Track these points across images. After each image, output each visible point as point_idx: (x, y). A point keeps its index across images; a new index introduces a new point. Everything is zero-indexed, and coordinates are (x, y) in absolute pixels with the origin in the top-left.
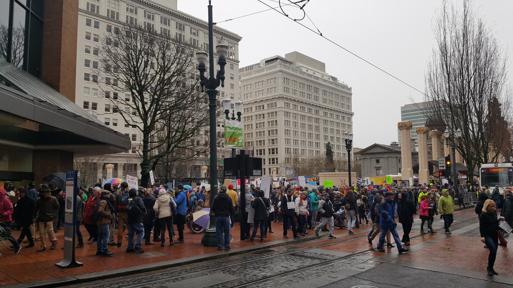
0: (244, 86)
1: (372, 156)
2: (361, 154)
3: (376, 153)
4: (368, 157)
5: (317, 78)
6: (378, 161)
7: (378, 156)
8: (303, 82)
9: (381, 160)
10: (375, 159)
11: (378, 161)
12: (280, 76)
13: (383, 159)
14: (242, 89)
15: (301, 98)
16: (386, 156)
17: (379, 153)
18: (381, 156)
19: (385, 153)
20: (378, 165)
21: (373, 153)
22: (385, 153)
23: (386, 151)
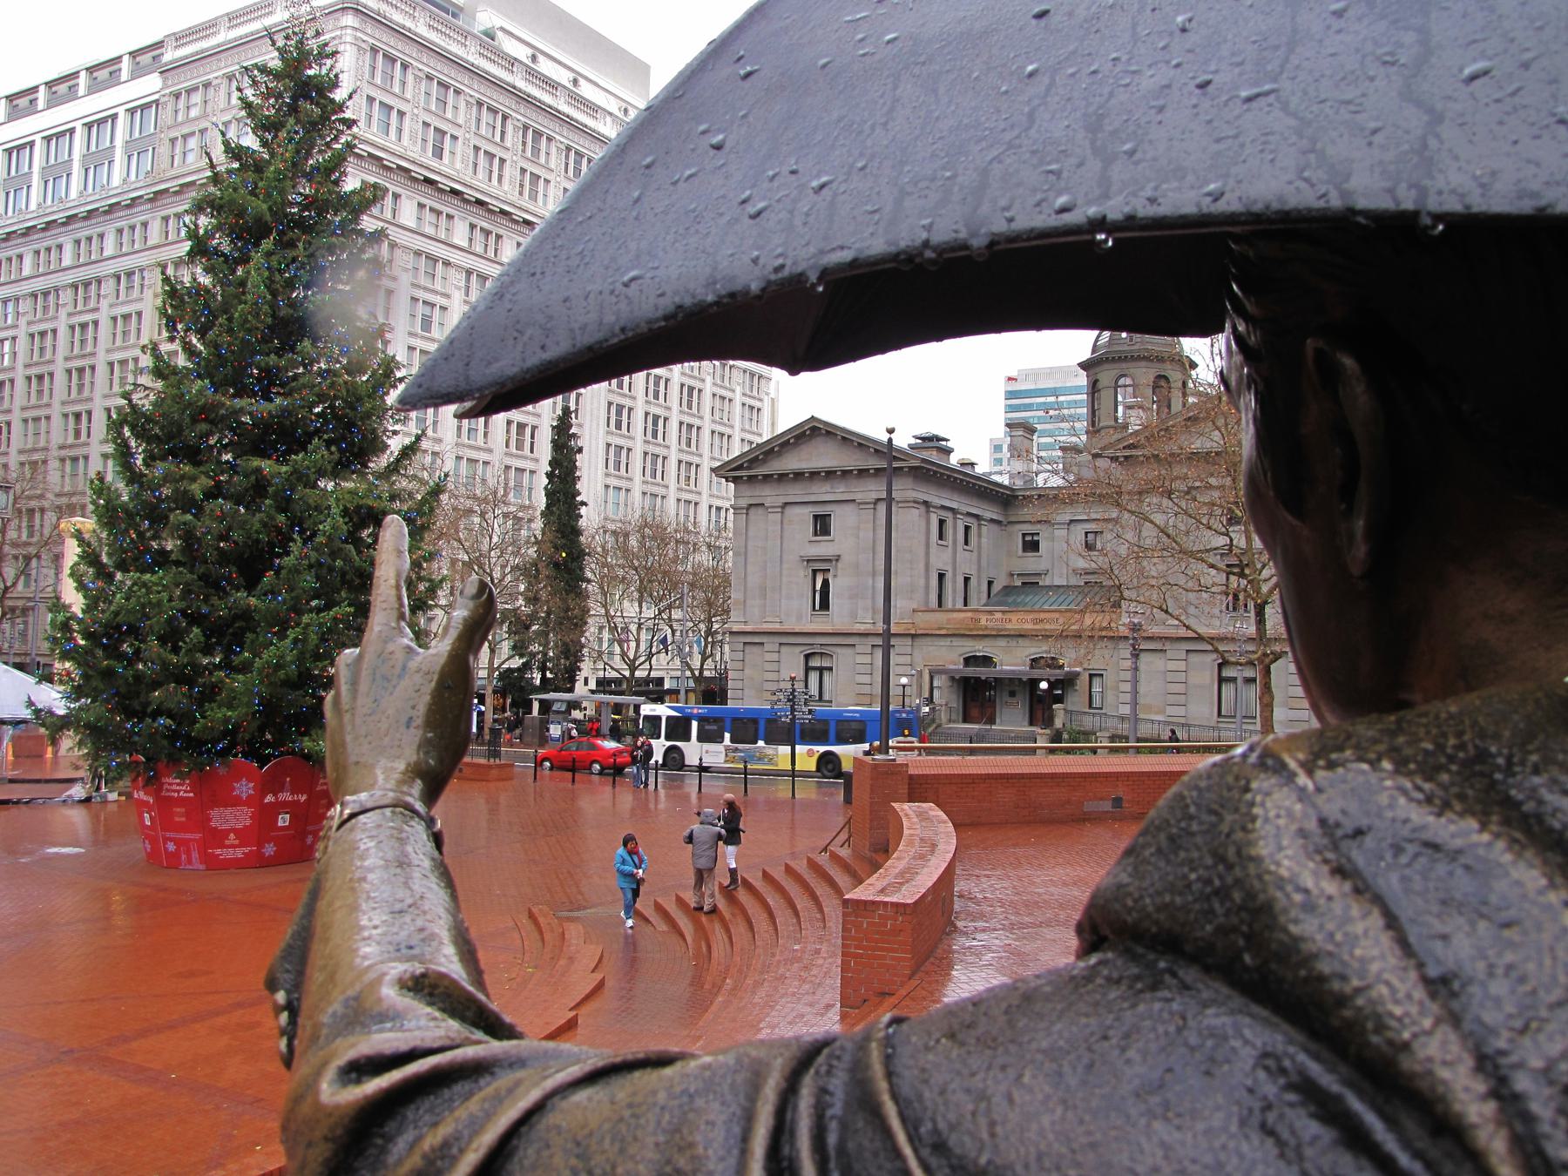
0: (177, 96)
1: (795, 492)
2: (735, 480)
3: (814, 475)
4: (771, 495)
5: (593, 109)
6: (822, 525)
7: (822, 491)
8: (504, 103)
9: (841, 519)
10: (807, 513)
11: (822, 525)
12: (349, 36)
13: (849, 508)
14: (167, 115)
15: (479, 183)
16: (873, 489)
17: (830, 474)
18: (839, 491)
19: (863, 473)
20: (823, 548)
21: (798, 476)
22: (863, 473)
23: (874, 463)
